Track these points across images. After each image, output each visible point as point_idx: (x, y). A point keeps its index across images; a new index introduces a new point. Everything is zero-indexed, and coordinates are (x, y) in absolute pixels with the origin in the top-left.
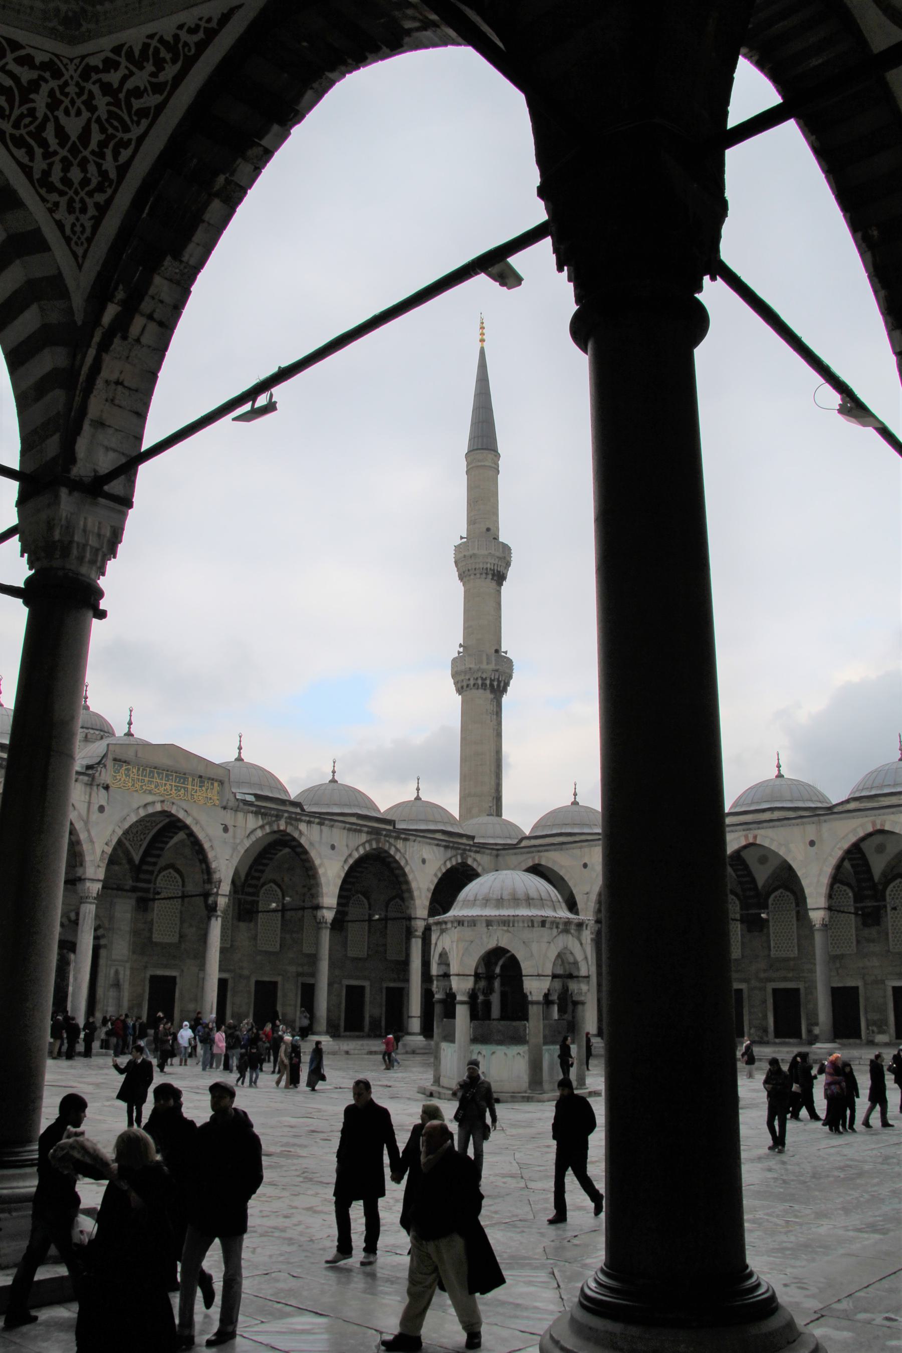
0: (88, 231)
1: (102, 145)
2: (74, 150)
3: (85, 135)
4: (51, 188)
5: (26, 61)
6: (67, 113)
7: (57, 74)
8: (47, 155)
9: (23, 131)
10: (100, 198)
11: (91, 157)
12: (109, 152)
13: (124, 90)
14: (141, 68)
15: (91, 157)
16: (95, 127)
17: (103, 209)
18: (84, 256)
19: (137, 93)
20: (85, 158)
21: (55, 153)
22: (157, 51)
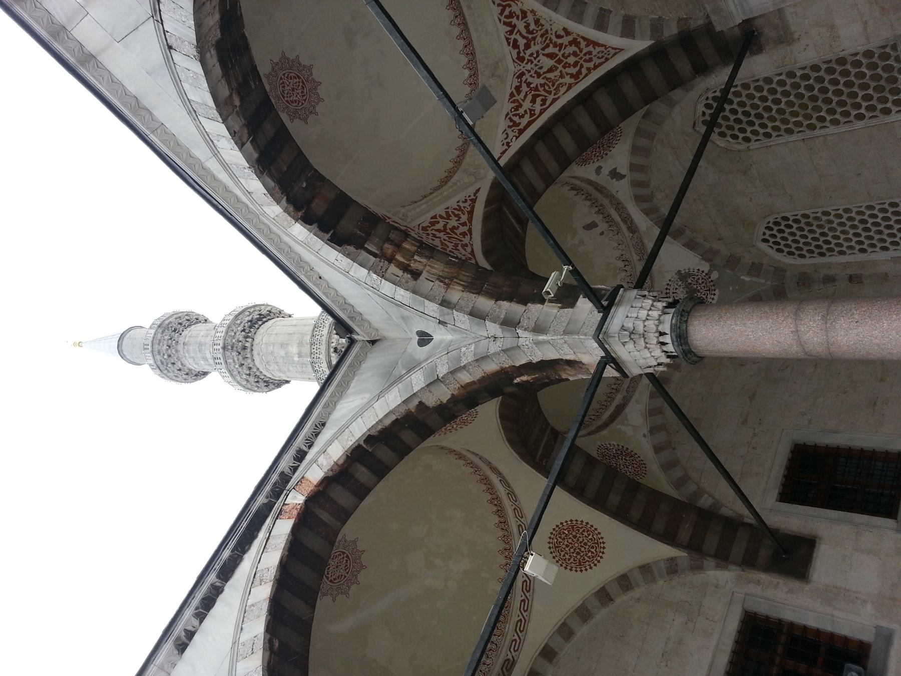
0: (602, 49)
1: (555, 45)
2: (559, 61)
3: (551, 56)
4: (579, 72)
5: (518, 89)
6: (541, 68)
7: (523, 74)
8: (562, 76)
9: (552, 89)
10: (583, 44)
11: (562, 52)
12: (559, 41)
13: (526, 35)
14: (515, 26)
15: (562, 52)
16: (547, 51)
17: (589, 42)
18: (616, 49)
19: (527, 27)
20: (563, 55)
21: (561, 72)
22: (506, 17)
